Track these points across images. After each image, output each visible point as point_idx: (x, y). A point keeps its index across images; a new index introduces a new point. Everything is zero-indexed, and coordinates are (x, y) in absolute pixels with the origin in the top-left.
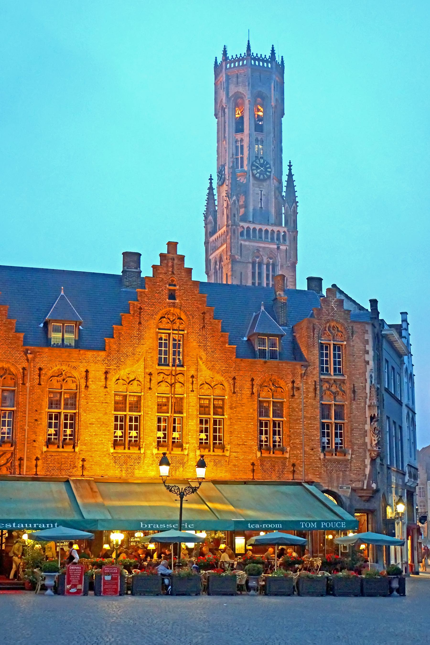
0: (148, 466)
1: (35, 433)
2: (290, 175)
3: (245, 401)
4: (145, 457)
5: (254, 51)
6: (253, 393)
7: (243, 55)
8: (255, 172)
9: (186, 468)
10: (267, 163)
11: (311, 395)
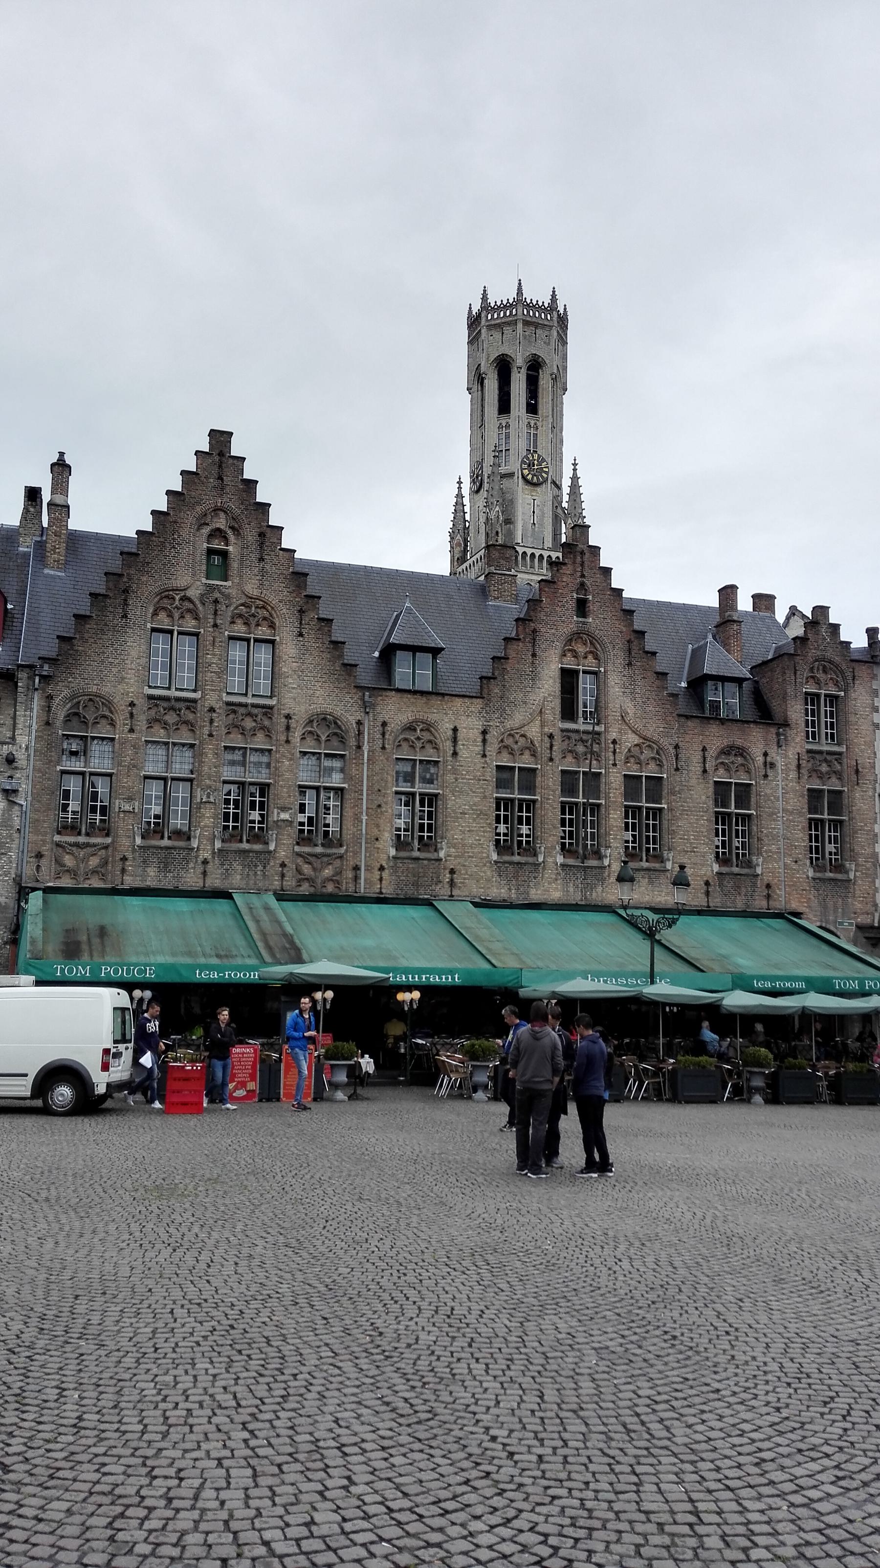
0: (550, 883)
1: (378, 826)
2: (575, 478)
3: (693, 782)
4: (544, 869)
5: (528, 295)
6: (705, 771)
7: (511, 301)
8: (526, 472)
10: (544, 460)
11: (793, 775)
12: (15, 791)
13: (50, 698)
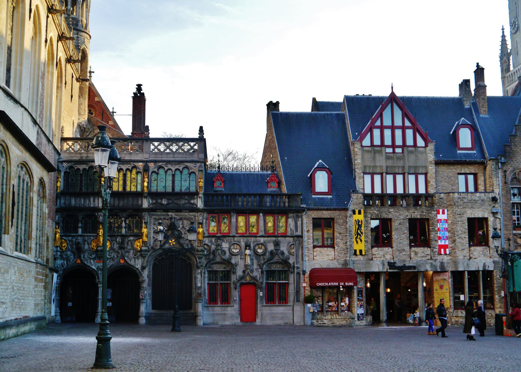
12: (497, 213)
13: (505, 172)
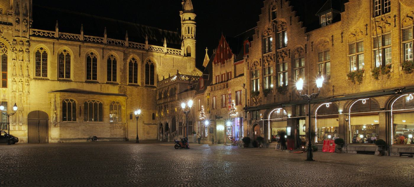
9: (392, 81)
